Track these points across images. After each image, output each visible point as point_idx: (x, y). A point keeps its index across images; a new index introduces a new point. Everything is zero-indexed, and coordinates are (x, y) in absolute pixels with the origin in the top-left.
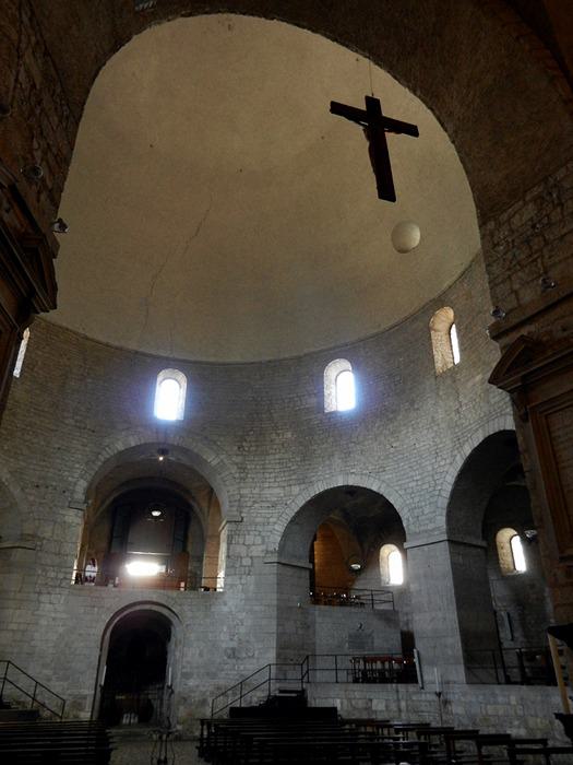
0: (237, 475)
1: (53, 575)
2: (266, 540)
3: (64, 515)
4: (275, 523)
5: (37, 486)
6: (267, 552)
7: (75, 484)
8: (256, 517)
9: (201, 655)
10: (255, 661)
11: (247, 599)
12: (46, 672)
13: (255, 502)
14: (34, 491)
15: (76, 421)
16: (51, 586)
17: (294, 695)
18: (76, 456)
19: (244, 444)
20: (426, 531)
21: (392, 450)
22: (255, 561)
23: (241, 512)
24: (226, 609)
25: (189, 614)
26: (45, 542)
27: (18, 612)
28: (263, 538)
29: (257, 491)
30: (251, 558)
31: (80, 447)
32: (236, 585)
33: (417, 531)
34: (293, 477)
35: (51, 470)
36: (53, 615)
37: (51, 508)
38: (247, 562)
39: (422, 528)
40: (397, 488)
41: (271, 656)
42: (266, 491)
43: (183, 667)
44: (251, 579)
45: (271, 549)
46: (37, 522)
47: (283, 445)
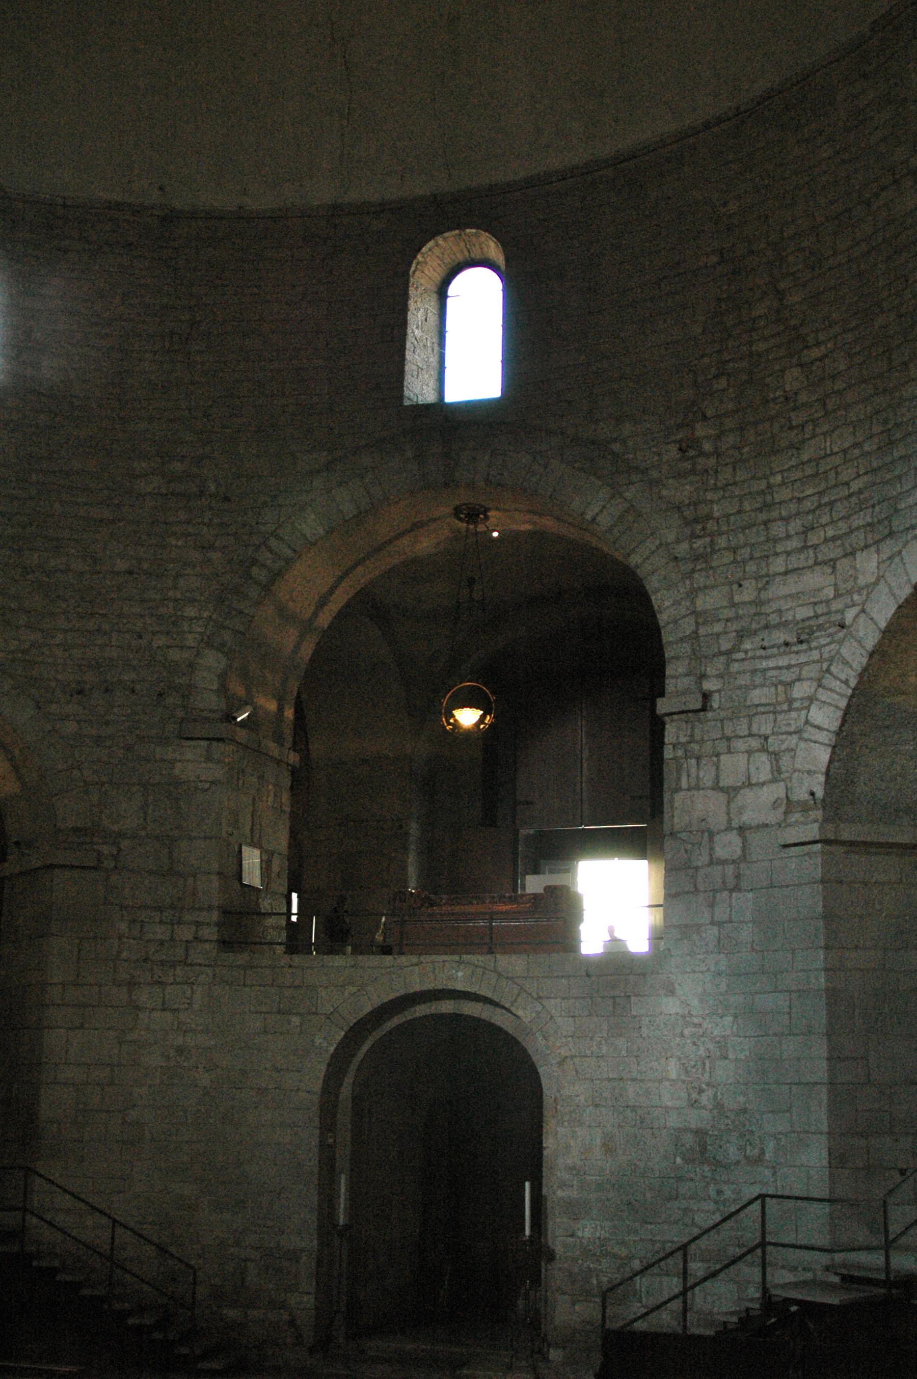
0: (683, 548)
1: (160, 932)
2: (785, 761)
3: (173, 762)
4: (811, 699)
5: (80, 692)
6: (790, 805)
9: (608, 1148)
10: (768, 1172)
13: (741, 635)
22: (755, 839)
23: (703, 676)
24: (671, 1006)
26: (125, 843)
28: (775, 756)
29: (747, 594)
32: (698, 927)
36: (180, 1041)
37: (129, 748)
42: (779, 589)
43: (563, 1185)
44: (745, 902)
45: (801, 794)
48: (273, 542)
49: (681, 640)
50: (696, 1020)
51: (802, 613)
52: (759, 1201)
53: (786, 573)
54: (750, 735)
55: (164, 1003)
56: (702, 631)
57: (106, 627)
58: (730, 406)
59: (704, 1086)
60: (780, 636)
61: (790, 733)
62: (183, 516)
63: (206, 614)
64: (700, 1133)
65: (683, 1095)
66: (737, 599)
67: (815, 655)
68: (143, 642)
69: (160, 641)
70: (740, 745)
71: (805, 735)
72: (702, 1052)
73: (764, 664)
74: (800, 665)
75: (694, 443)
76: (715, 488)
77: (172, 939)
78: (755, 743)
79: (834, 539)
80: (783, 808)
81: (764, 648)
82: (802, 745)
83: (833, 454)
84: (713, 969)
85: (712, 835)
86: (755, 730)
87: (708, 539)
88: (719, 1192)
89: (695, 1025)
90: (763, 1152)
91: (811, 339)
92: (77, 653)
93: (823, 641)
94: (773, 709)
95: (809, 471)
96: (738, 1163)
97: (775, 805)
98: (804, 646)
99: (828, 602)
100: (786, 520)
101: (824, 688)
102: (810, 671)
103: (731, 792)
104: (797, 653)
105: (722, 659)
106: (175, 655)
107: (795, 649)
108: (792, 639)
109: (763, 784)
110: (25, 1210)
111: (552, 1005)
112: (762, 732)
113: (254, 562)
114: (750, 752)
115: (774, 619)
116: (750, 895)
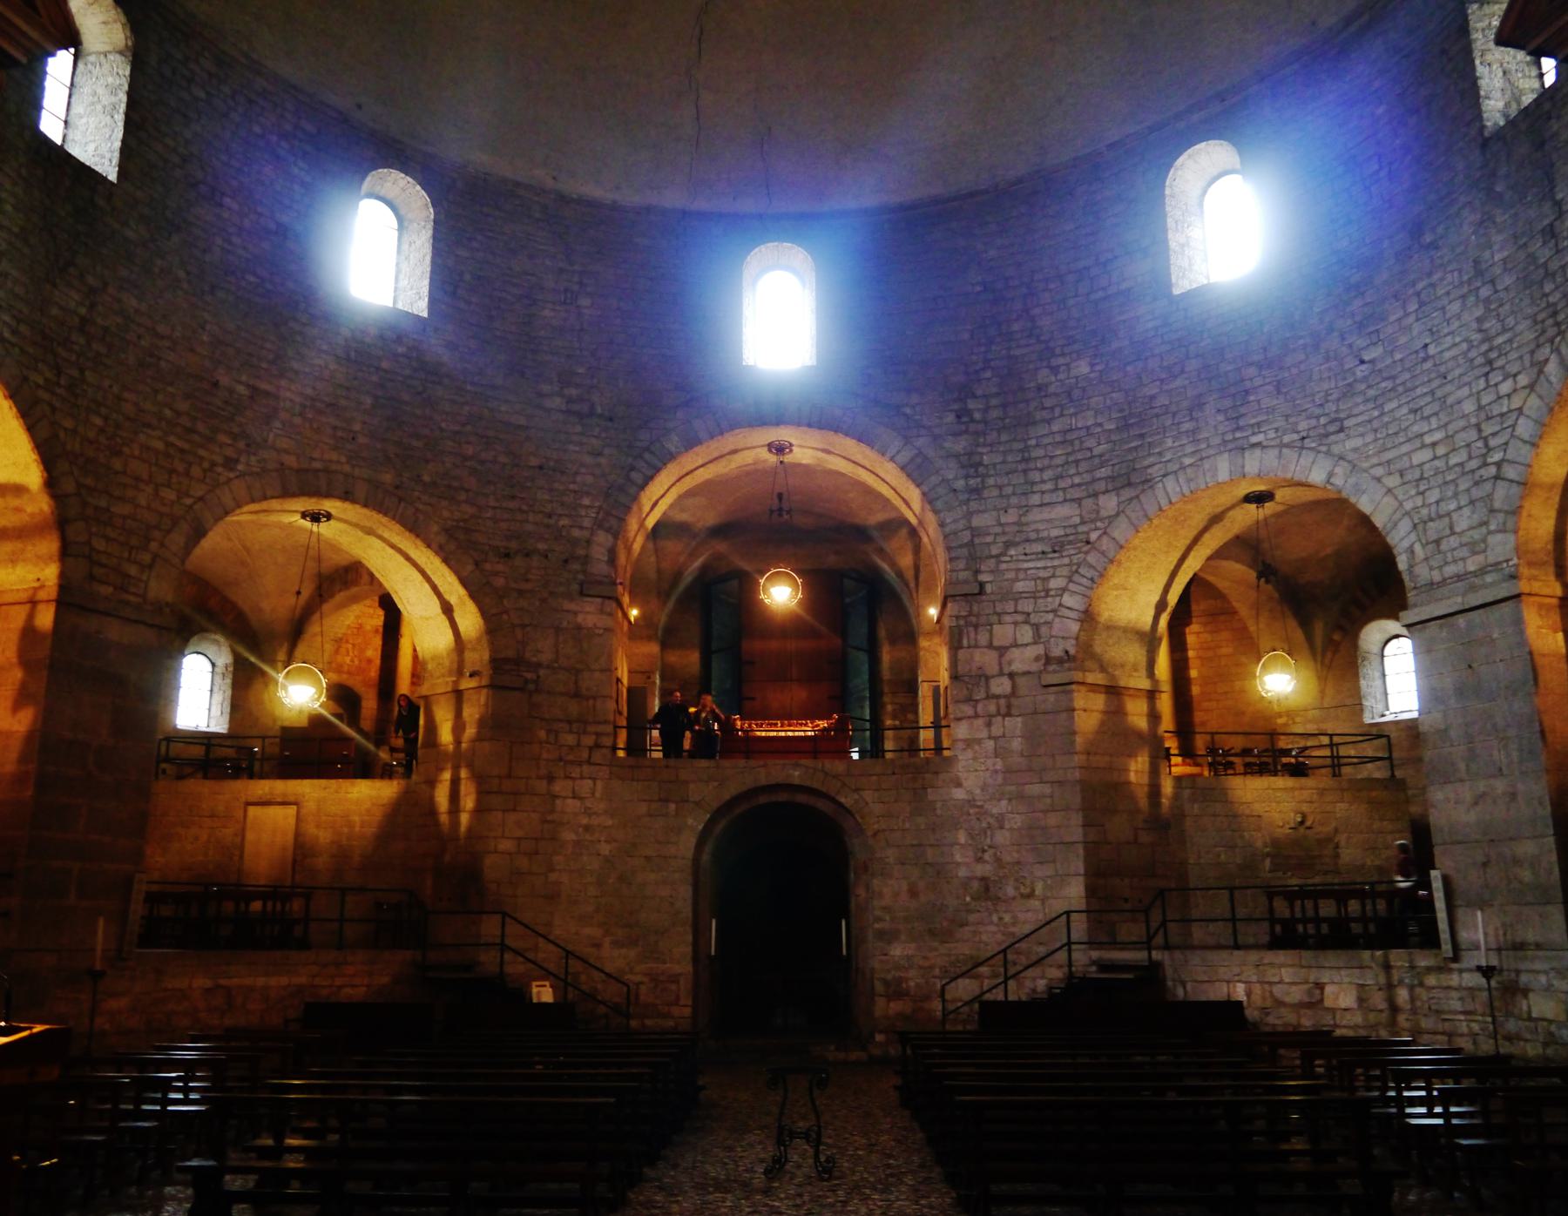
0: (960, 484)
1: (570, 739)
2: (1044, 630)
3: (575, 613)
4: (1064, 590)
5: (507, 555)
6: (1048, 660)
7: (588, 542)
8: (1017, 580)
9: (913, 893)
10: (1037, 903)
11: (1008, 771)
12: (588, 931)
13: (1008, 545)
14: (500, 567)
15: (570, 400)
16: (572, 762)
17: (1130, 976)
18: (579, 479)
19: (971, 404)
20: (1459, 577)
21: (1362, 371)
22: (1021, 681)
23: (977, 572)
24: (959, 794)
25: (877, 808)
26: (542, 672)
27: (512, 818)
28: (1036, 627)
29: (1011, 517)
30: (1011, 676)
31: (588, 459)
32: (979, 741)
33: (1437, 576)
34: (1103, 472)
35: (531, 517)
36: (585, 821)
37: (544, 600)
38: (1001, 686)
39: (1450, 570)
40: (1379, 471)
41: (1074, 892)
42: (1035, 515)
43: (879, 919)
44: (1015, 724)
46: (519, 632)
47: (1069, 394)
48: (647, 456)
49: (961, 546)
50: (979, 803)
51: (1055, 533)
52: (1065, 916)
53: (1041, 505)
54: (1016, 612)
55: (574, 792)
56: (977, 541)
57: (525, 508)
58: (994, 390)
59: (986, 848)
60: (1039, 548)
61: (1047, 612)
62: (579, 429)
63: (597, 504)
64: (983, 879)
65: (971, 853)
66: (1003, 520)
67: (1066, 561)
68: (552, 521)
69: (564, 522)
70: (1008, 618)
71: (1059, 613)
72: (984, 825)
73: (1026, 565)
74: (1054, 567)
75: (969, 413)
76: (985, 445)
77: (578, 745)
78: (1020, 618)
79: (1079, 485)
80: (1043, 661)
81: (1026, 554)
82: (1057, 620)
83: (1077, 429)
84: (991, 768)
85: (987, 678)
86: (1020, 608)
87: (979, 480)
88: (1001, 919)
89: (978, 807)
90: (1033, 891)
91: (1058, 351)
92: (504, 525)
93: (1072, 552)
94: (1034, 596)
95: (1058, 438)
96: (1014, 898)
97: (1037, 659)
98: (1056, 555)
99: (1075, 526)
100: (1041, 470)
101: (1074, 582)
102: (1065, 571)
103: (1002, 650)
104: (1051, 559)
105: (993, 560)
106: (576, 533)
107: (1050, 556)
108: (1048, 549)
109: (1027, 645)
110: (503, 947)
111: (868, 795)
112: (1026, 610)
113: (632, 468)
114: (1016, 623)
115: (1033, 536)
116: (1019, 719)
